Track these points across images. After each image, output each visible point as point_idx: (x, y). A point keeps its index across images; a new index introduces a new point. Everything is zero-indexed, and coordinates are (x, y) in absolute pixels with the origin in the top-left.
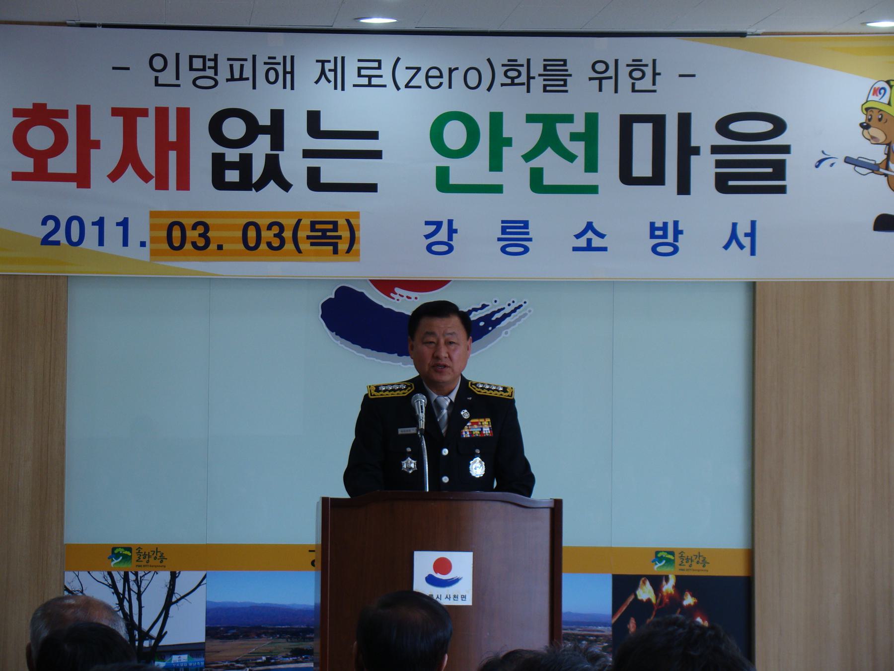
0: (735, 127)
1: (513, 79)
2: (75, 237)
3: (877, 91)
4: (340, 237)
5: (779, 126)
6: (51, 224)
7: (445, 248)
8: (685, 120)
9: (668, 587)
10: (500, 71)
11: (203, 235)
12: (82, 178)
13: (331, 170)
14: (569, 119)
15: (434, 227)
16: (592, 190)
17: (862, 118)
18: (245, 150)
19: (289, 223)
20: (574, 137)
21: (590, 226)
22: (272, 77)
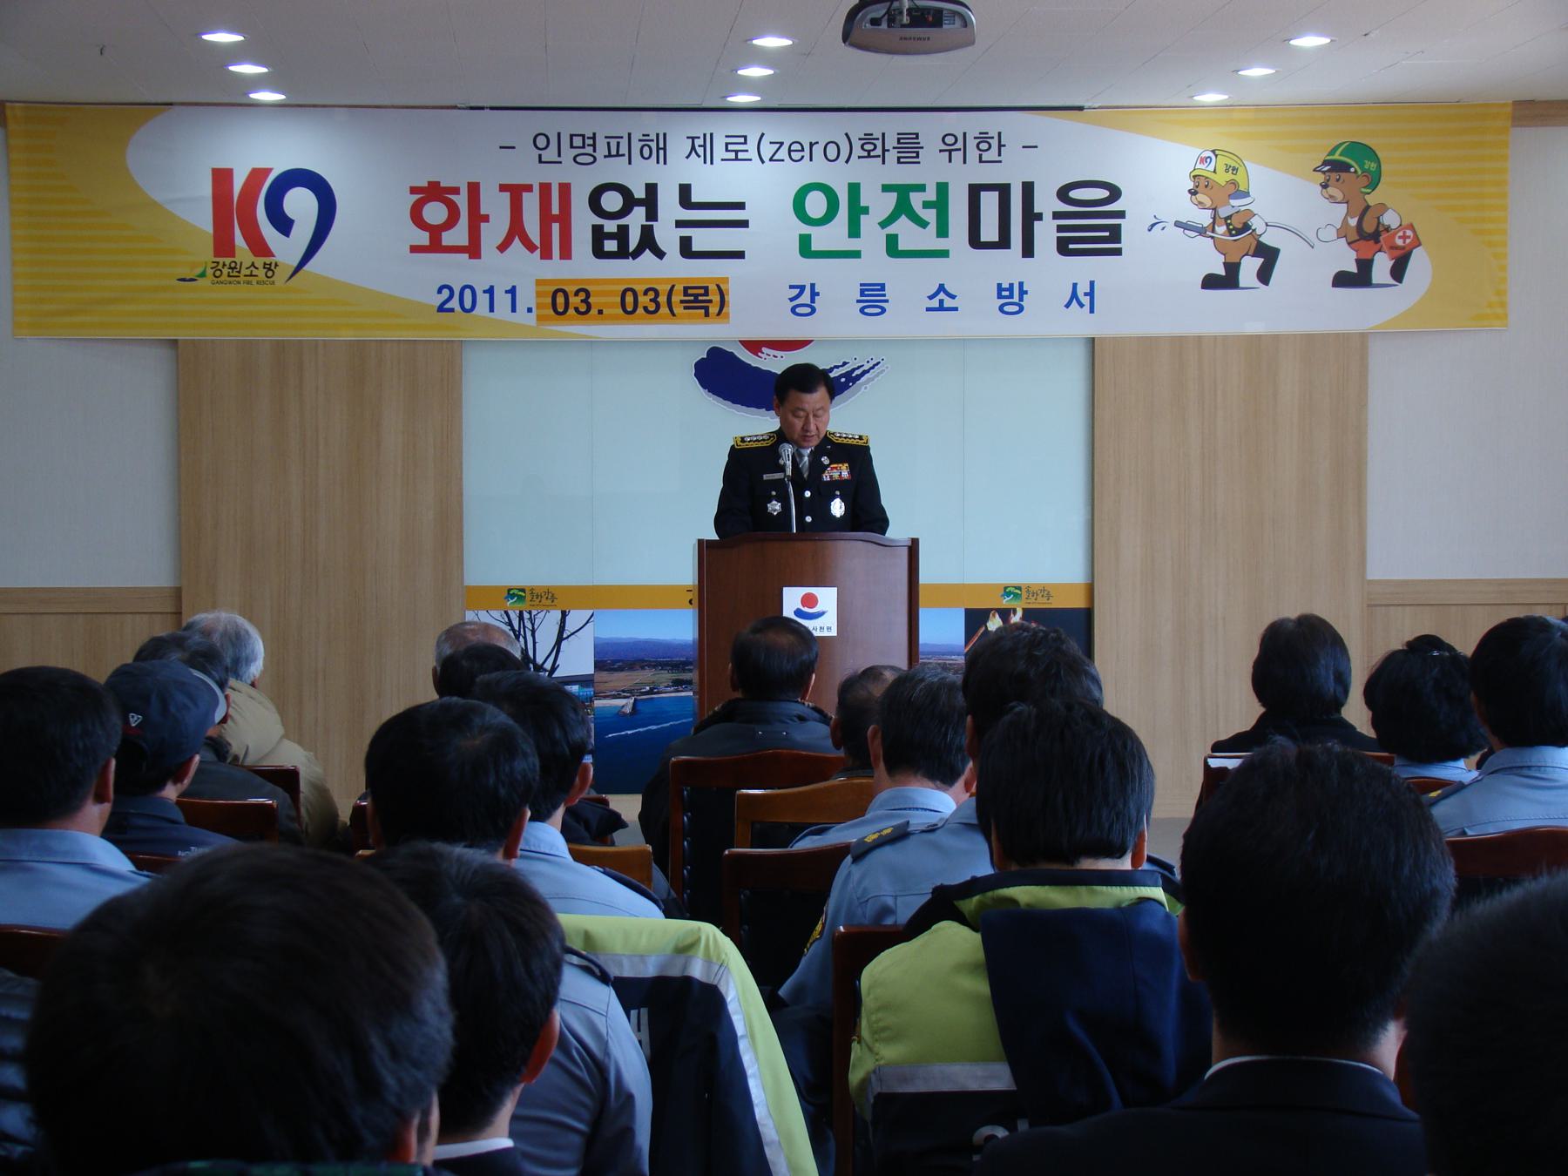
0: (1074, 194)
1: (869, 151)
2: (468, 305)
3: (1203, 160)
4: (710, 301)
5: (1115, 193)
6: (446, 293)
7: (808, 310)
8: (1028, 189)
9: (1016, 619)
10: (857, 145)
11: (585, 301)
12: (473, 250)
13: (703, 240)
14: (921, 188)
15: (797, 291)
16: (944, 254)
17: (1191, 185)
18: (622, 222)
19: (663, 289)
20: (926, 205)
21: (941, 288)
22: (646, 152)
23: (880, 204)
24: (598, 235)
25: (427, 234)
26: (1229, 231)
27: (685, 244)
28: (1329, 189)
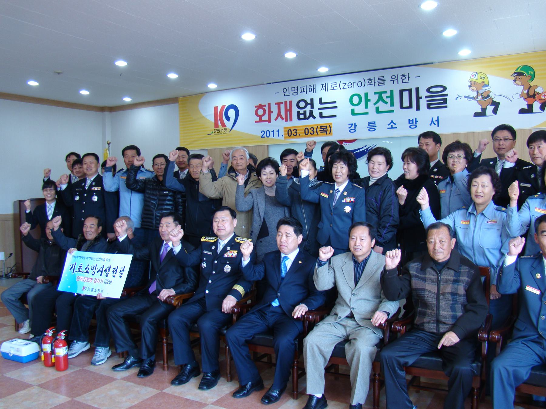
0: (432, 90)
1: (370, 83)
2: (268, 136)
4: (327, 130)
5: (445, 88)
7: (354, 131)
8: (417, 90)
10: (367, 81)
12: (269, 121)
13: (325, 113)
14: (385, 92)
15: (351, 125)
16: (393, 111)
17: (469, 84)
18: (305, 110)
19: (315, 127)
20: (387, 97)
22: (310, 90)
23: (373, 98)
24: (299, 113)
25: (259, 118)
26: (483, 98)
27: (321, 114)
28: (516, 82)
